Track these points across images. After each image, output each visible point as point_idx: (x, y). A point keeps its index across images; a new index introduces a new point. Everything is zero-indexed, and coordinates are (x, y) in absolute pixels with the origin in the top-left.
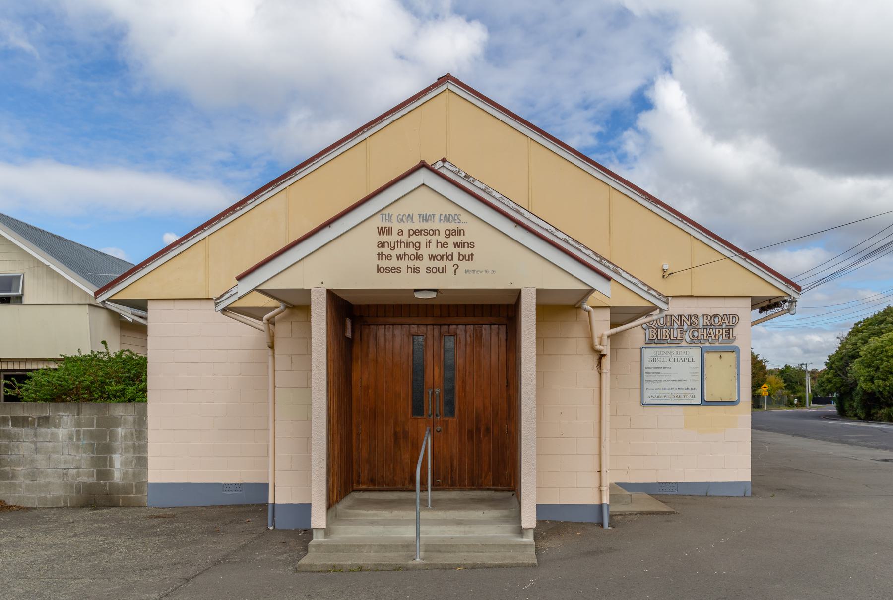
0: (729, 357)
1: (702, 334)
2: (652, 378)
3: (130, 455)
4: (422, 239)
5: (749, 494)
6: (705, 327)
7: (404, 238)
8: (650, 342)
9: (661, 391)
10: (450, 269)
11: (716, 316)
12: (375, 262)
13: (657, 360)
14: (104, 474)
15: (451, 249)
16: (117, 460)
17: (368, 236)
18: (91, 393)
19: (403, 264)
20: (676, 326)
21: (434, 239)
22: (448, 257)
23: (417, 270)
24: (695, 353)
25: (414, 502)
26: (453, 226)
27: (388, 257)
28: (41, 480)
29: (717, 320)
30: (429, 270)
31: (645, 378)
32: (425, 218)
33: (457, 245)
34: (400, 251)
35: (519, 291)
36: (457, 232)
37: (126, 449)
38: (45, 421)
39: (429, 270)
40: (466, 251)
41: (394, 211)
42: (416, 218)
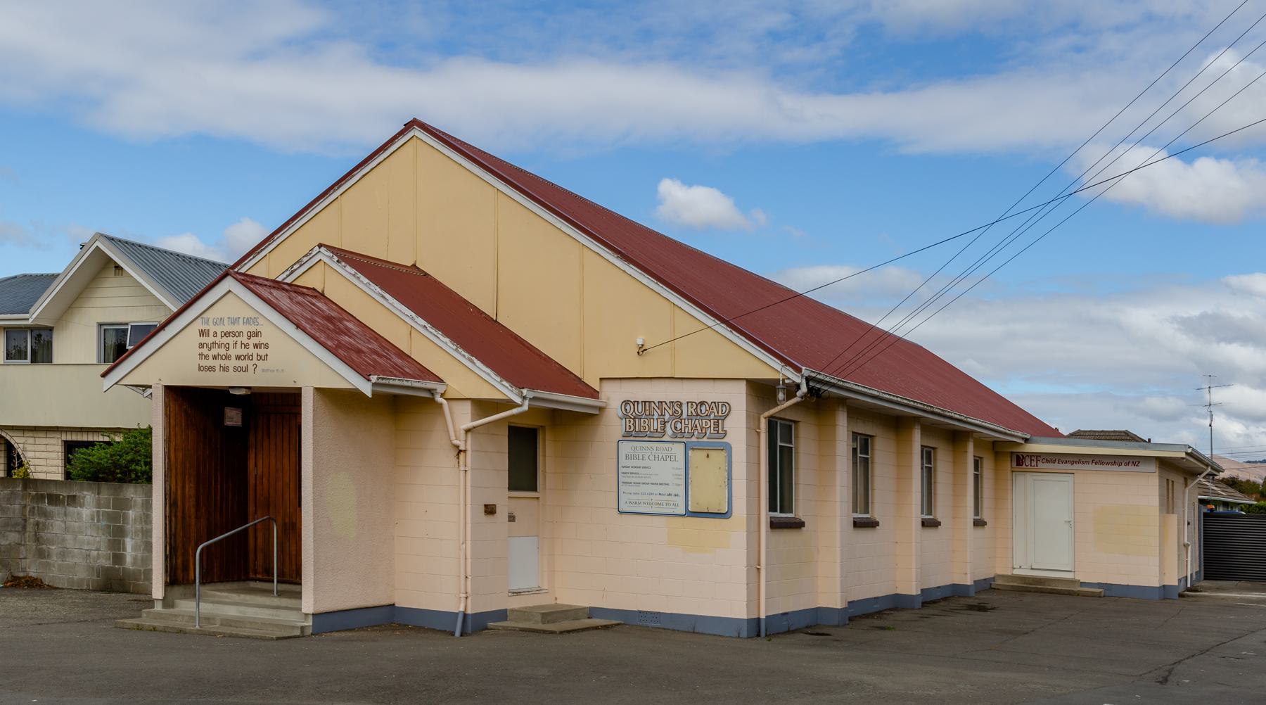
0: (718, 457)
1: (686, 426)
2: (629, 480)
3: (139, 539)
4: (230, 340)
5: (744, 634)
6: (690, 417)
7: (218, 340)
8: (628, 435)
9: (640, 497)
10: (251, 368)
11: (702, 403)
12: (197, 362)
13: (635, 457)
14: (118, 558)
15: (251, 350)
16: (129, 543)
17: (192, 335)
18: (124, 473)
19: (217, 363)
20: (656, 416)
21: (239, 339)
22: (249, 357)
23: (226, 369)
24: (678, 449)
25: (272, 592)
26: (253, 328)
27: (206, 357)
28: (70, 561)
29: (703, 408)
30: (236, 369)
31: (622, 479)
32: (233, 321)
33: (256, 346)
34: (215, 351)
35: (300, 389)
36: (256, 334)
37: (136, 533)
38: (73, 500)
39: (236, 369)
40: (262, 352)
41: (210, 315)
42: (226, 321)
